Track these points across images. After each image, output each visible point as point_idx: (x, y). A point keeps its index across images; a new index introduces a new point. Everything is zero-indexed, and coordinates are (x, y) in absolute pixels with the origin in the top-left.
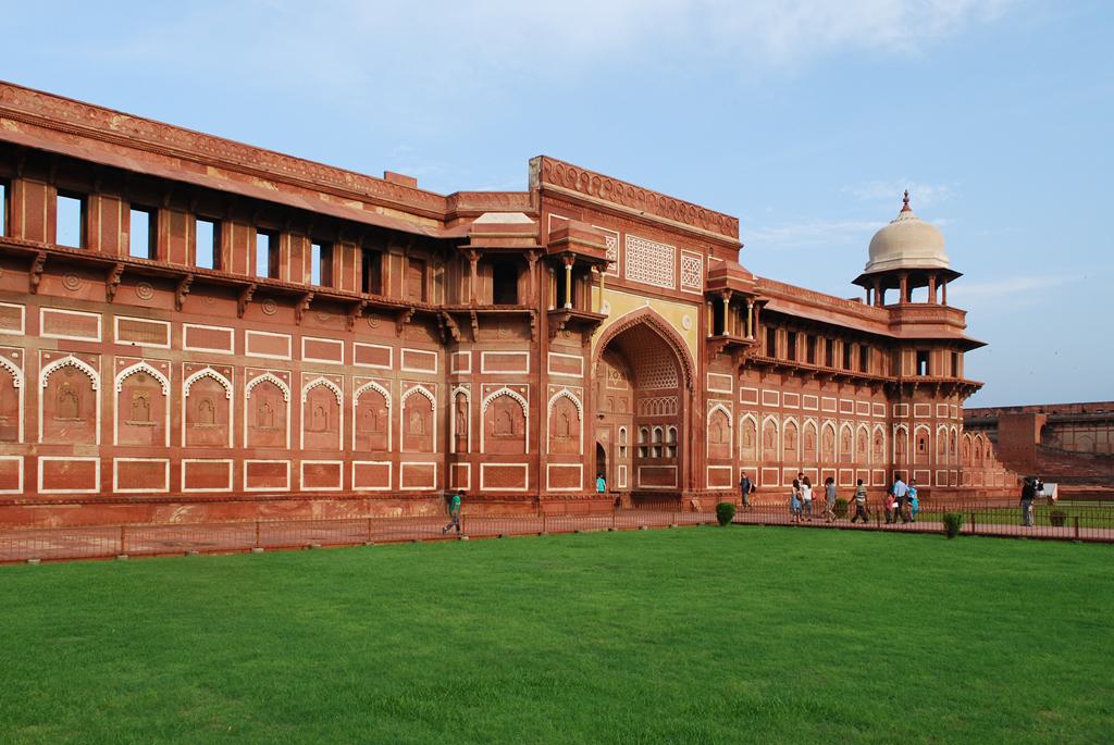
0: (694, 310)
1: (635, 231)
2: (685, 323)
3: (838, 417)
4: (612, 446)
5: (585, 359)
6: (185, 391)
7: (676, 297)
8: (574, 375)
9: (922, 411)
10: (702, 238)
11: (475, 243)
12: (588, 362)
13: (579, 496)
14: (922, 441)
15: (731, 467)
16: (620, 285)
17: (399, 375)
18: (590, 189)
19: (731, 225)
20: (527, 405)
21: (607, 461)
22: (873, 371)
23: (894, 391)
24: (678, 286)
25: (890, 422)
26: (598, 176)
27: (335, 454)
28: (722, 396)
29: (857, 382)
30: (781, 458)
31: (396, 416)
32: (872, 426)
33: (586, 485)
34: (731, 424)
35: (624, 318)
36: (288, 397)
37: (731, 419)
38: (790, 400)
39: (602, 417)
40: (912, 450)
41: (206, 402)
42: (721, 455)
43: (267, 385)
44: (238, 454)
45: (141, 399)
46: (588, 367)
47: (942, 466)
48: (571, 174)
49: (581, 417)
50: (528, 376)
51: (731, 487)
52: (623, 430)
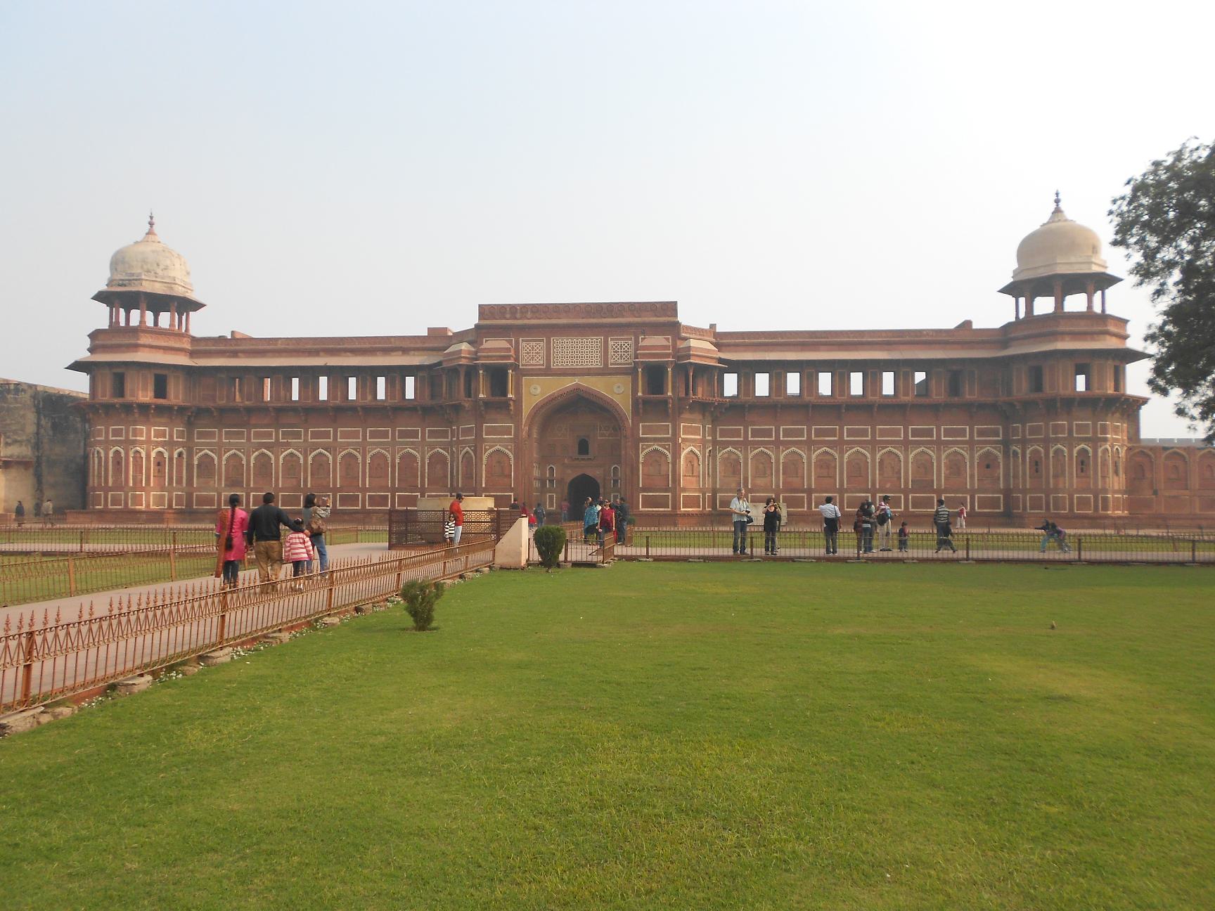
0: (629, 378)
1: (561, 335)
2: (618, 392)
3: (906, 444)
6: (310, 461)
7: (605, 372)
9: (1034, 431)
10: (629, 325)
11: (444, 365)
14: (1037, 464)
16: (547, 372)
17: (421, 445)
18: (518, 315)
19: (671, 308)
21: (601, 490)
22: (971, 394)
23: (1005, 413)
24: (606, 364)
25: (1006, 444)
26: (524, 306)
27: (386, 489)
28: (655, 440)
29: (934, 410)
30: (809, 484)
31: (423, 466)
32: (972, 449)
36: (360, 460)
38: (818, 433)
40: (1024, 473)
41: (320, 464)
43: (350, 454)
44: (335, 490)
45: (291, 465)
46: (518, 428)
47: (1056, 490)
48: (500, 311)
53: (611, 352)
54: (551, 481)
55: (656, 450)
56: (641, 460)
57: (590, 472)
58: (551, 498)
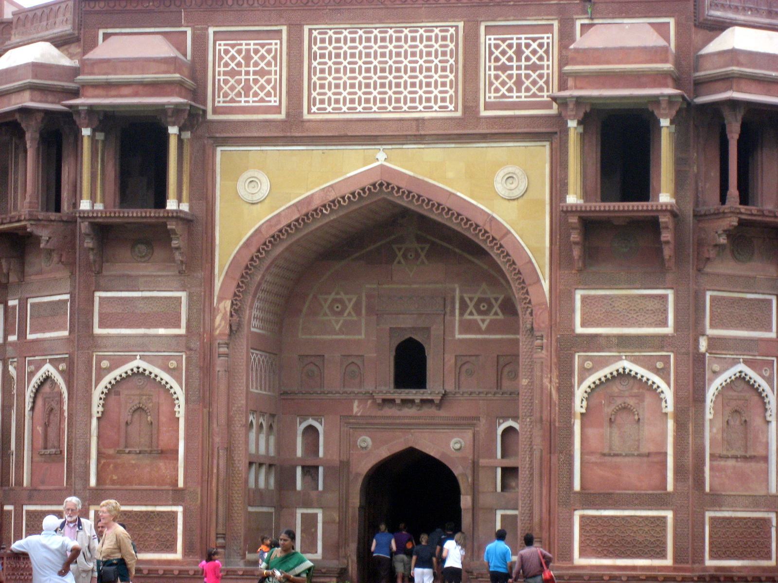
0: (542, 152)
4: (475, 465)
5: (190, 297)
8: (162, 331)
12: (202, 305)
13: (176, 568)
15: (669, 515)
16: (292, 131)
20: (65, 395)
21: (466, 501)
28: (624, 343)
33: (188, 549)
34: (669, 406)
35: (309, 199)
37: (669, 394)
39: (431, 401)
42: (633, 476)
49: (181, 411)
50: (68, 340)
51: (668, 562)
52: (509, 431)
53: (486, 69)
54: (310, 471)
55: (623, 376)
56: (579, 406)
57: (430, 444)
58: (309, 522)
